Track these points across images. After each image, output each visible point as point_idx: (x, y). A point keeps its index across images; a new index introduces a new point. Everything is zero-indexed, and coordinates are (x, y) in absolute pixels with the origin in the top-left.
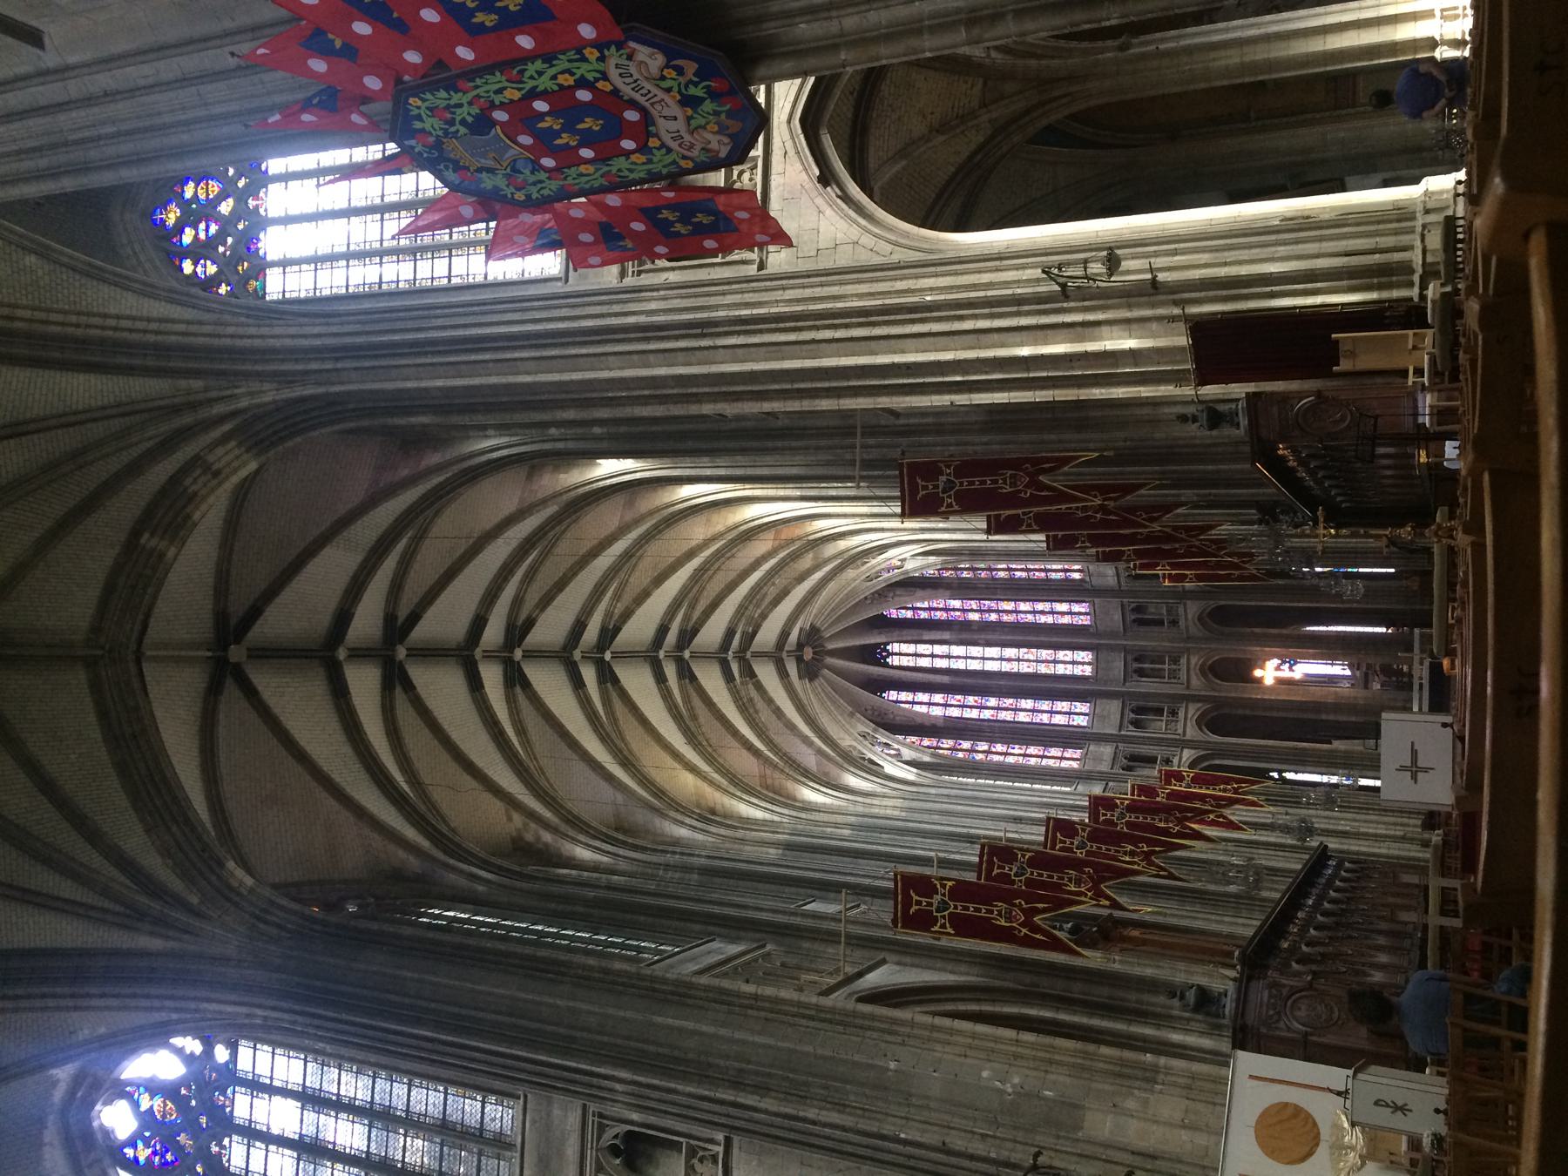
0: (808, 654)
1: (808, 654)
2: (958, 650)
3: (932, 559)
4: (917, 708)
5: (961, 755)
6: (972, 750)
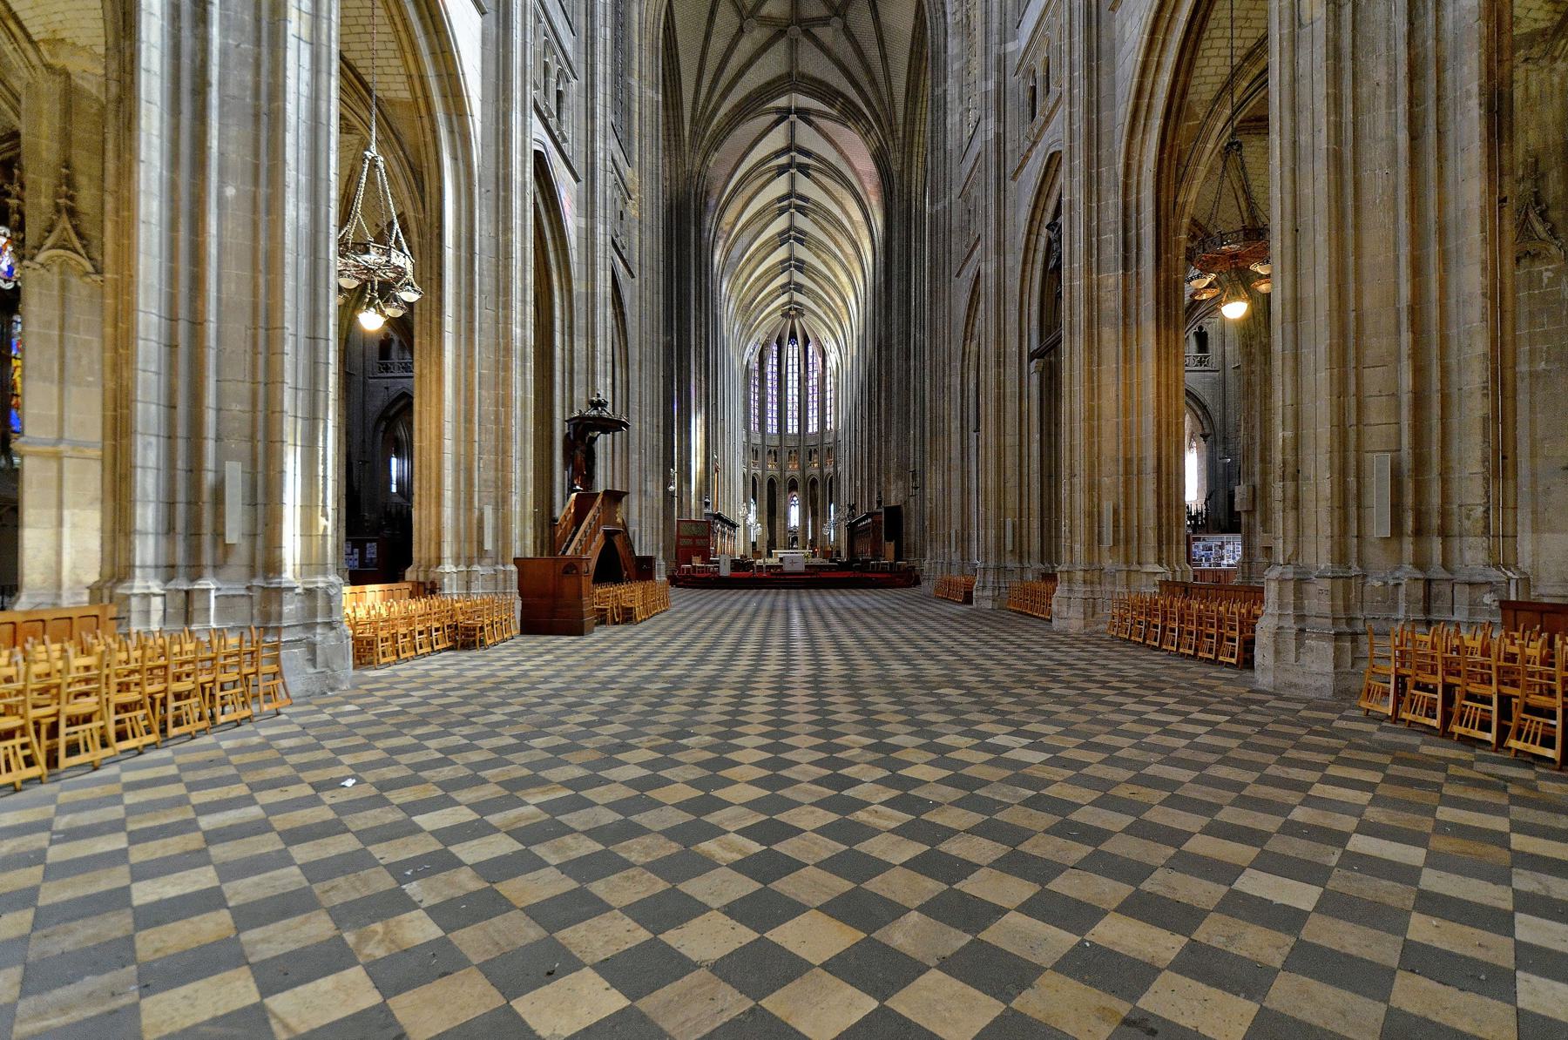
1: (793, 312)
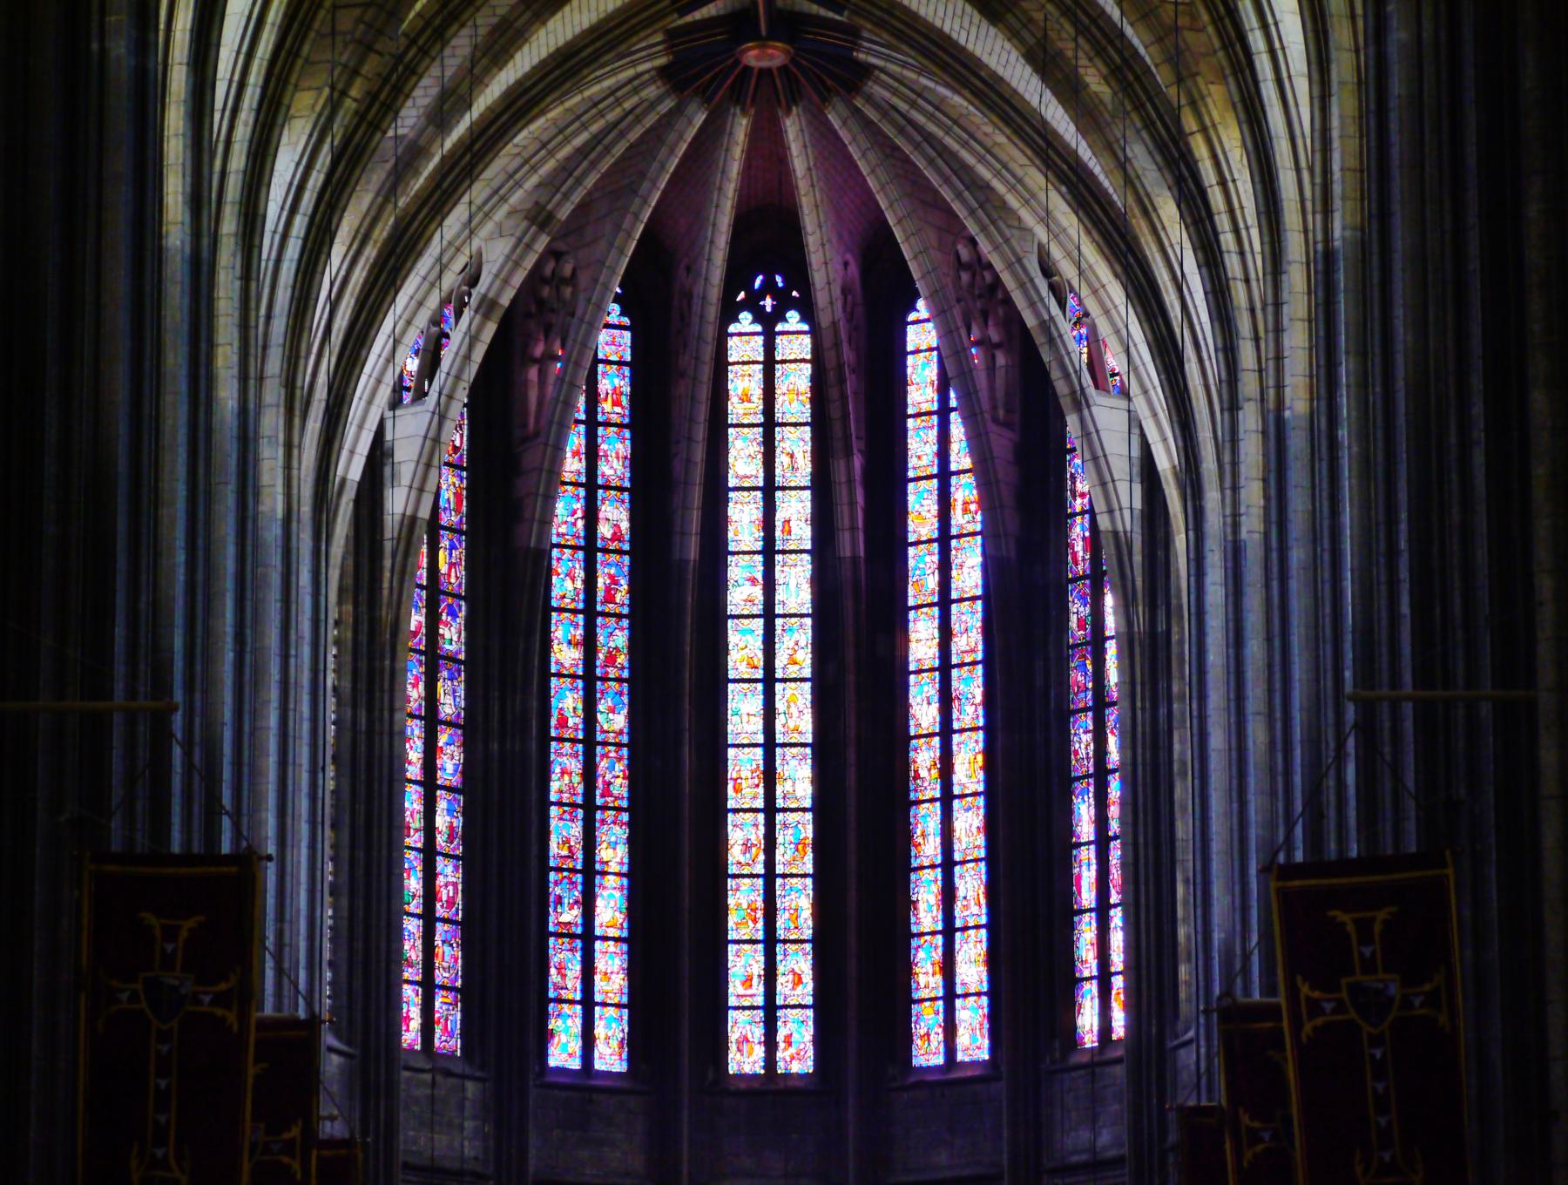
0: (761, 57)
2: (796, 586)
3: (1130, 496)
4: (576, 439)
5: (417, 619)
6: (434, 659)
